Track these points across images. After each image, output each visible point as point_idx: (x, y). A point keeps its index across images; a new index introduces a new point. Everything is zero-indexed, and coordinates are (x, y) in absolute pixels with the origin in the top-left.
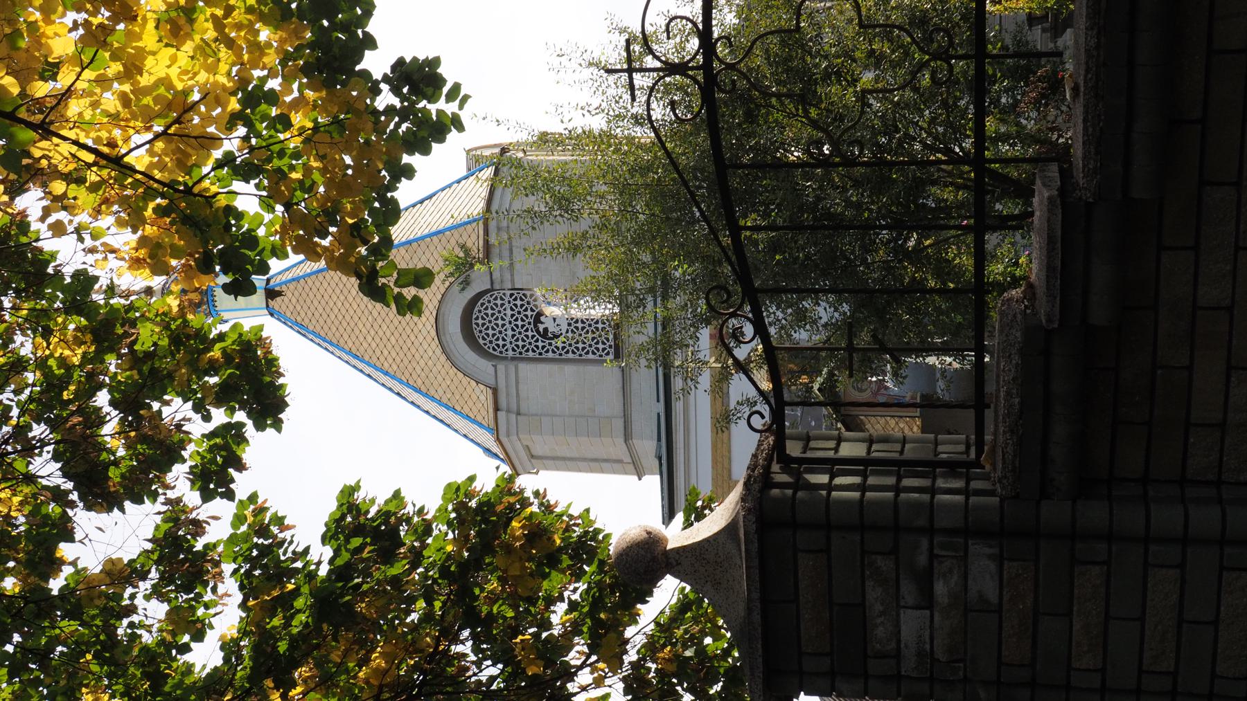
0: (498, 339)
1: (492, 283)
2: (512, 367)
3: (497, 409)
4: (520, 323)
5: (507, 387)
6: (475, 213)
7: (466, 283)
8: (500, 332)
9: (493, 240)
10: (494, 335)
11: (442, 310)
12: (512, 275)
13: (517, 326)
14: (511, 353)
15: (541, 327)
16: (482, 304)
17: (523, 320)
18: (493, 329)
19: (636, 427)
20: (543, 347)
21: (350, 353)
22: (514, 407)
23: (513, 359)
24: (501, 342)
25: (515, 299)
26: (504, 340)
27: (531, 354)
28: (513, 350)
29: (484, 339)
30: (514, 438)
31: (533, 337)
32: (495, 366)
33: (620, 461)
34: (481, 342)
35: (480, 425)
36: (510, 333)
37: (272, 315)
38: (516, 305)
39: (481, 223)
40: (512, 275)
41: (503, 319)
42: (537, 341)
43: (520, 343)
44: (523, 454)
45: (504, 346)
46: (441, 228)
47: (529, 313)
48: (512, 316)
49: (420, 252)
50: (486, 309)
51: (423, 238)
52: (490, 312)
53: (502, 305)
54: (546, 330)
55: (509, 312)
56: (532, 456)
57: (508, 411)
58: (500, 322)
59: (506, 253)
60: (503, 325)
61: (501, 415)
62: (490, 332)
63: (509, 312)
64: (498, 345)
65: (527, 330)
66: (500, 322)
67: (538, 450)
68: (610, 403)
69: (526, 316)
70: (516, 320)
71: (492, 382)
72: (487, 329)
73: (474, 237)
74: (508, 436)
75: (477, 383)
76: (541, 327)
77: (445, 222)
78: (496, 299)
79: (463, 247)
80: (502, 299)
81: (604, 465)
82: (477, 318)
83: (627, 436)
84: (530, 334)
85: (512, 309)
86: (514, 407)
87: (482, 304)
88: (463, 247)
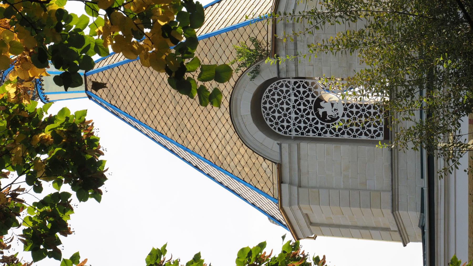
0: (283, 121)
1: (279, 73)
2: (294, 146)
3: (281, 182)
4: (302, 107)
5: (290, 162)
6: (266, 11)
7: (256, 72)
8: (285, 115)
9: (280, 35)
10: (279, 117)
11: (235, 97)
12: (296, 66)
13: (300, 110)
14: (294, 133)
15: (321, 111)
16: (270, 91)
17: (305, 105)
18: (279, 112)
19: (402, 200)
20: (322, 129)
21: (156, 131)
22: (296, 180)
23: (296, 138)
24: (285, 124)
25: (299, 87)
26: (288, 122)
27: (311, 134)
28: (296, 131)
29: (271, 121)
30: (295, 207)
31: (314, 119)
32: (280, 145)
33: (387, 229)
34: (268, 123)
35: (267, 195)
36: (293, 116)
37: (90, 97)
38: (299, 92)
39: (271, 20)
40: (296, 66)
41: (288, 104)
42: (317, 123)
43: (302, 125)
44: (303, 221)
45: (288, 127)
46: (235, 24)
47: (310, 99)
48: (296, 101)
49: (217, 45)
50: (273, 94)
51: (219, 33)
52: (276, 97)
53: (287, 91)
54: (325, 113)
55: (293, 98)
56: (311, 224)
57: (291, 184)
58: (285, 106)
59: (291, 47)
60: (288, 109)
61: (285, 187)
62: (277, 115)
63: (293, 98)
64: (283, 127)
65: (308, 114)
66: (285, 106)
67: (315, 218)
68: (379, 177)
69: (308, 101)
70: (299, 104)
71: (277, 158)
72: (274, 112)
73: (264, 33)
74: (290, 205)
75: (265, 159)
76: (321, 111)
77: (239, 19)
78: (282, 86)
79: (254, 40)
80: (287, 86)
81: (373, 232)
82: (265, 103)
83: (394, 208)
84: (311, 117)
85: (295, 95)
86: (296, 180)
87: (270, 91)
88: (254, 40)
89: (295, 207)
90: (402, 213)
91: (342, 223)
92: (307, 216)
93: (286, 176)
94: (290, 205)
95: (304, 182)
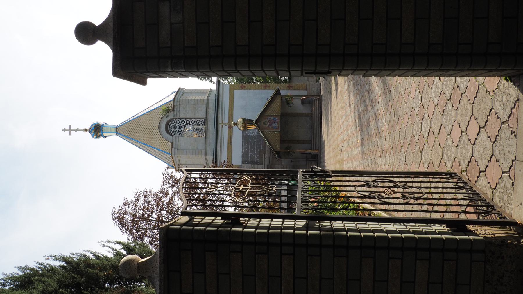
7: (168, 116)
9: (175, 104)
19: (208, 152)
30: (176, 156)
35: (167, 153)
59: (178, 108)
61: (173, 149)
68: (201, 146)
74: (174, 155)
83: (205, 154)
89: (176, 156)
90: (208, 156)
91: (190, 163)
92: (179, 160)
93: (174, 146)
94: (174, 155)
95: (179, 148)
